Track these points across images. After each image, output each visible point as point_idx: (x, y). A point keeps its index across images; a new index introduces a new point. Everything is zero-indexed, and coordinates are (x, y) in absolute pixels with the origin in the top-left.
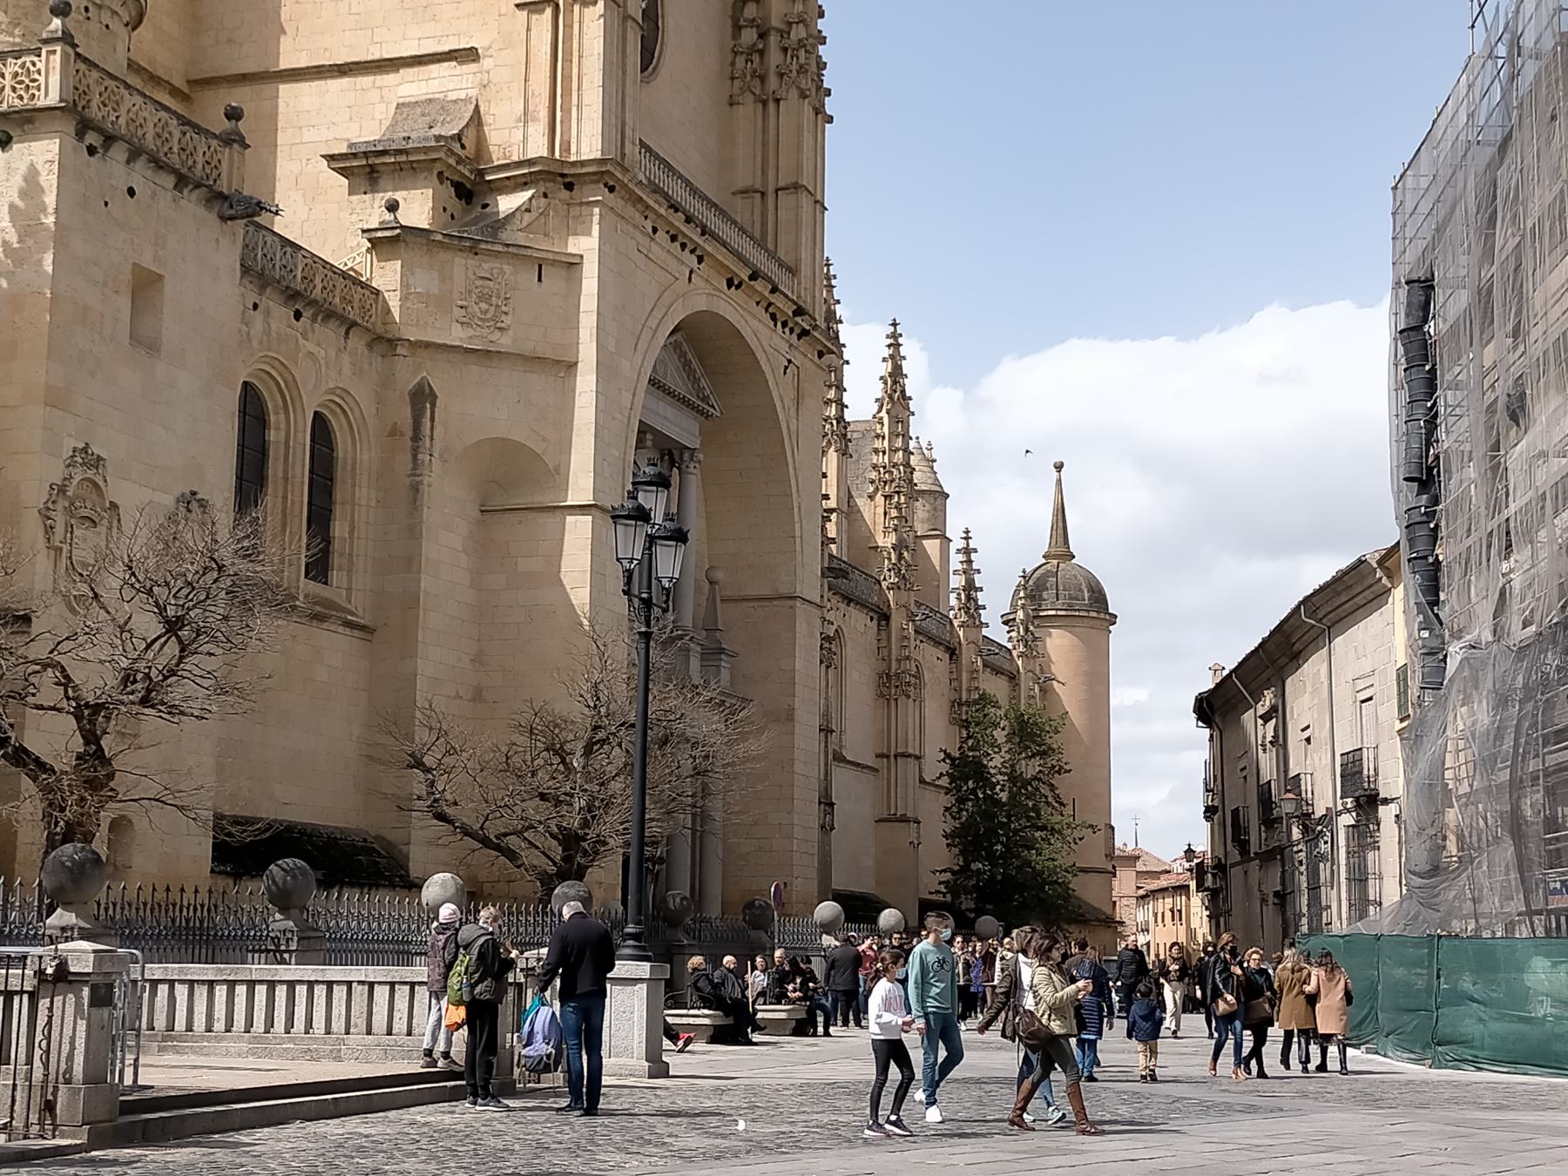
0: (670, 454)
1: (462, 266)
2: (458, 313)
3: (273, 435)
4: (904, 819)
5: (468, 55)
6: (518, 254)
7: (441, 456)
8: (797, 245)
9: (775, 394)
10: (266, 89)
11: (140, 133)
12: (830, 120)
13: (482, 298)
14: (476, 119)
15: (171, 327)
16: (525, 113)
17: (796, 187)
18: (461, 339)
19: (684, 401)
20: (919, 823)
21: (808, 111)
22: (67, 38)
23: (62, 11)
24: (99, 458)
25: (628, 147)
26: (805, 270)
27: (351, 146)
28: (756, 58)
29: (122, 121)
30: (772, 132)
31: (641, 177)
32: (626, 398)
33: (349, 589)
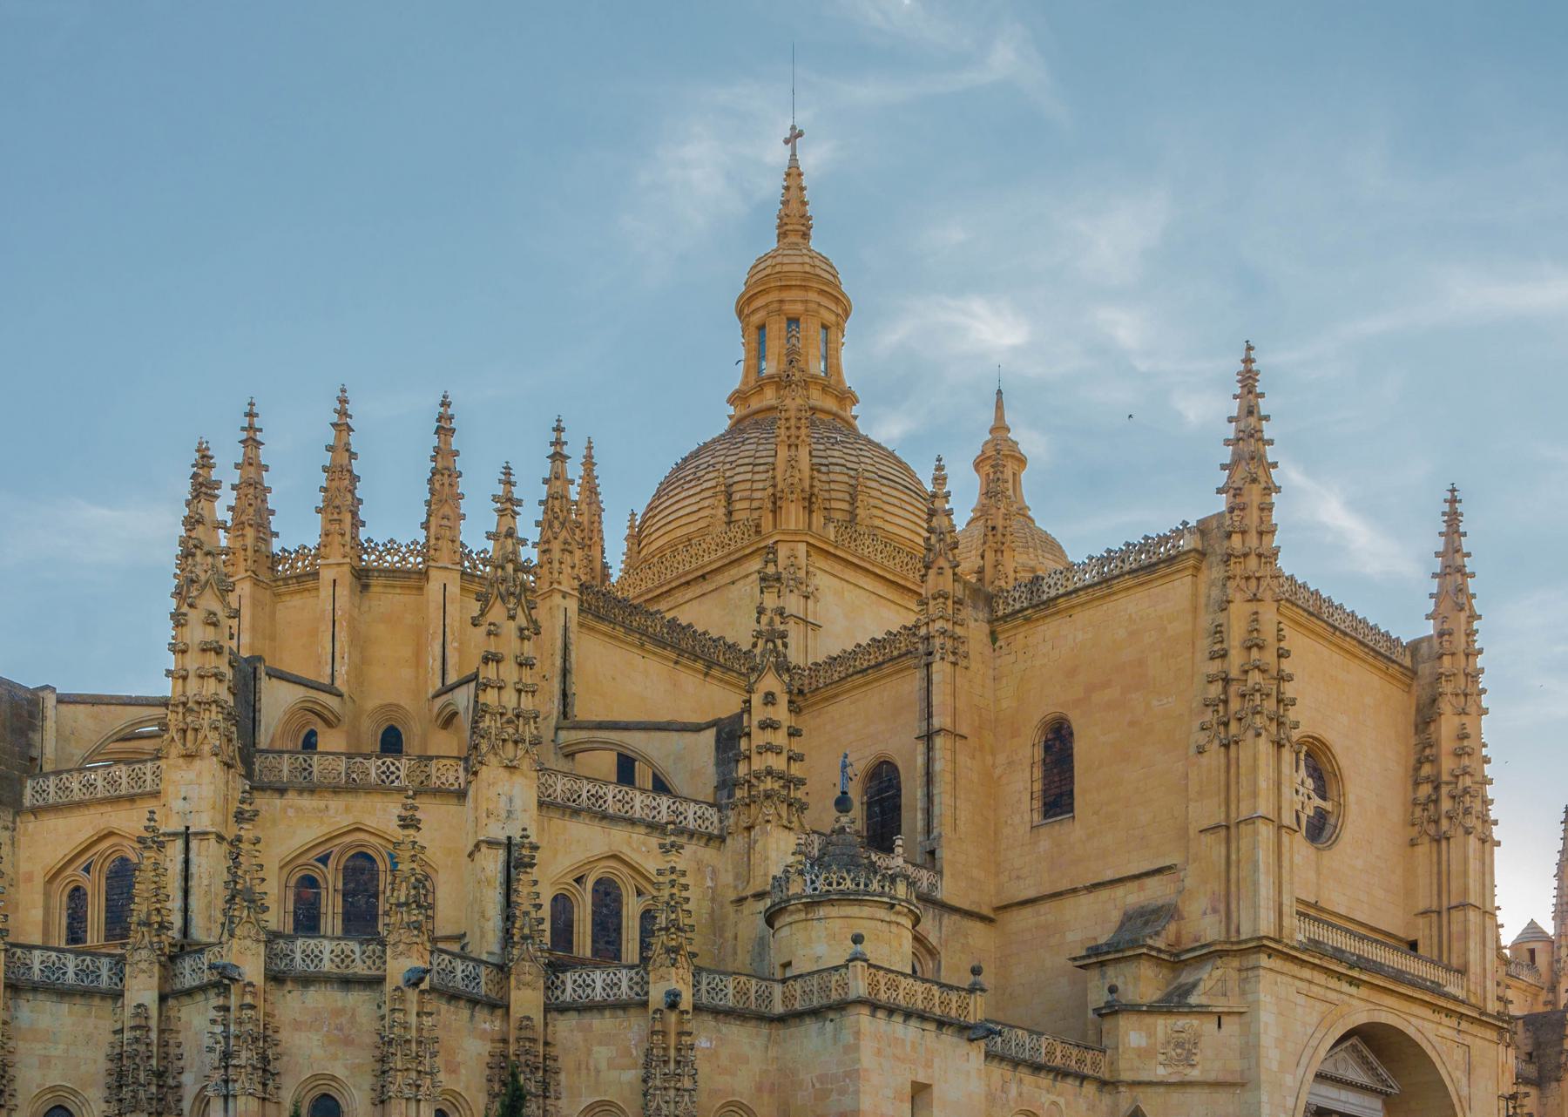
11: (913, 1000)
23: (858, 939)
29: (901, 997)
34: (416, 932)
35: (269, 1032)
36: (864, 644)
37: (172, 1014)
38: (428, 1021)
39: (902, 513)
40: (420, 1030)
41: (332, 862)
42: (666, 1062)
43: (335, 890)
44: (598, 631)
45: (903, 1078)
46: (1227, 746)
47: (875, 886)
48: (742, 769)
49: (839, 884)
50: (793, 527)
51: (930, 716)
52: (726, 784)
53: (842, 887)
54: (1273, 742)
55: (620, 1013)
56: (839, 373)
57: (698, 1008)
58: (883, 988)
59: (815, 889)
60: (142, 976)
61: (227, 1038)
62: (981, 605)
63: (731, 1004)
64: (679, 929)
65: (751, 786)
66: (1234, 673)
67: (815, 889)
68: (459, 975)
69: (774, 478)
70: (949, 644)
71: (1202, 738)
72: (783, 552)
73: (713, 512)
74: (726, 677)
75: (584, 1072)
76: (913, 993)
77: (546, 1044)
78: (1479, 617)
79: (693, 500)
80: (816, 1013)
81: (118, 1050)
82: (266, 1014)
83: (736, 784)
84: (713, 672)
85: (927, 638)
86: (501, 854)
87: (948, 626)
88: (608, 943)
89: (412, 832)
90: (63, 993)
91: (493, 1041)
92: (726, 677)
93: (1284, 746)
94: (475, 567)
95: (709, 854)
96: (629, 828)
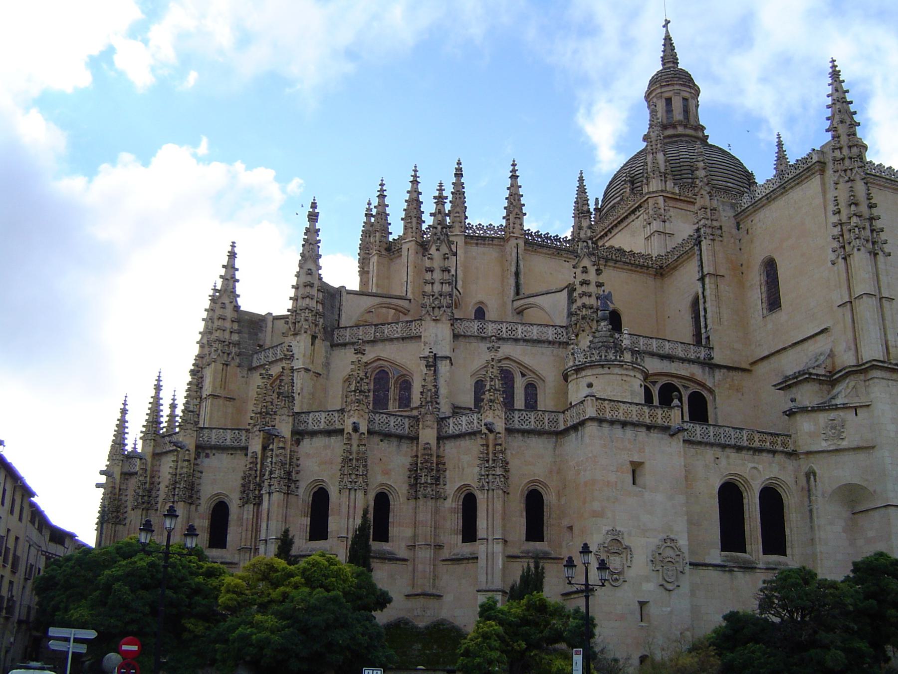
1: (822, 418)
6: (845, 407)
7: (823, 495)
13: (834, 428)
14: (831, 355)
15: (647, 477)
18: (825, 447)
23: (590, 385)
24: (620, 531)
34: (357, 404)
35: (294, 460)
36: (686, 239)
38: (363, 448)
40: (358, 453)
42: (488, 461)
44: (541, 253)
45: (625, 458)
46: (845, 259)
47: (611, 356)
48: (574, 306)
49: (591, 357)
52: (570, 314)
53: (593, 359)
54: (870, 253)
55: (473, 437)
57: (510, 431)
59: (580, 361)
60: (257, 438)
61: (272, 464)
63: (533, 427)
64: (496, 390)
65: (577, 315)
66: (844, 220)
67: (580, 361)
68: (392, 424)
70: (709, 231)
71: (832, 256)
72: (651, 201)
74: (617, 265)
77: (438, 457)
79: (618, 187)
80: (575, 428)
82: (291, 451)
84: (609, 264)
87: (709, 222)
89: (359, 355)
90: (221, 448)
91: (412, 457)
92: (617, 265)
93: (878, 254)
94: (475, 232)
95: (561, 352)
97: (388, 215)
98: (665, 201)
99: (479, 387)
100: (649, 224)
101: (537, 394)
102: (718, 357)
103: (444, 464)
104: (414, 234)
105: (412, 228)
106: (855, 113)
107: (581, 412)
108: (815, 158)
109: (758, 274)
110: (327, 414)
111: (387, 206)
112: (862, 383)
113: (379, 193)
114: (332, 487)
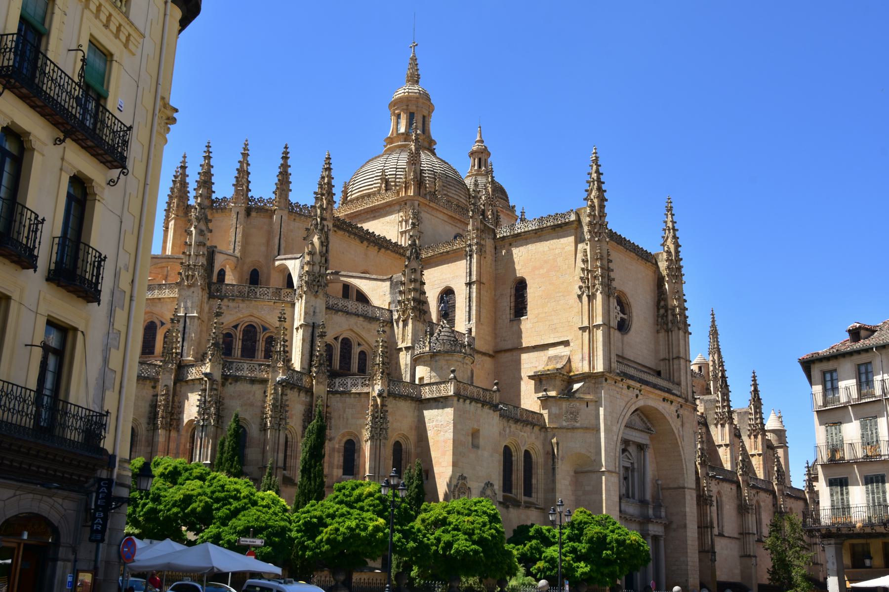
0: (640, 446)
1: (564, 405)
2: (564, 418)
3: (513, 458)
4: (750, 556)
5: (566, 343)
8: (680, 376)
9: (673, 425)
10: (515, 353)
12: (691, 334)
13: (571, 413)
14: (569, 361)
15: (482, 442)
16: (582, 358)
17: (678, 358)
19: (641, 431)
20: (755, 557)
21: (681, 332)
22: (455, 378)
23: (453, 372)
25: (613, 365)
26: (683, 383)
27: (534, 372)
28: (665, 318)
30: (670, 341)
31: (618, 371)
32: (615, 438)
33: (537, 498)
35: (221, 400)
37: (178, 389)
38: (285, 398)
39: (453, 188)
40: (282, 402)
41: (239, 328)
43: (239, 339)
46: (588, 296)
50: (412, 194)
51: (470, 275)
56: (429, 133)
57: (390, 394)
58: (462, 391)
62: (491, 233)
68: (295, 378)
69: (406, 175)
73: (379, 185)
75: (342, 419)
76: (470, 391)
77: (327, 406)
78: (680, 246)
81: (154, 403)
82: (220, 393)
83: (399, 302)
85: (470, 245)
86: (310, 329)
88: (345, 364)
91: (306, 405)
96: (357, 318)
97: (213, 175)
98: (419, 205)
99: (329, 348)
100: (406, 222)
101: (366, 360)
102: (478, 345)
103: (330, 413)
104: (244, 200)
105: (243, 195)
106: (605, 191)
107: (442, 388)
108: (573, 217)
109: (510, 287)
110: (249, 365)
111: (212, 167)
112: (593, 385)
113: (205, 155)
114: (253, 425)
